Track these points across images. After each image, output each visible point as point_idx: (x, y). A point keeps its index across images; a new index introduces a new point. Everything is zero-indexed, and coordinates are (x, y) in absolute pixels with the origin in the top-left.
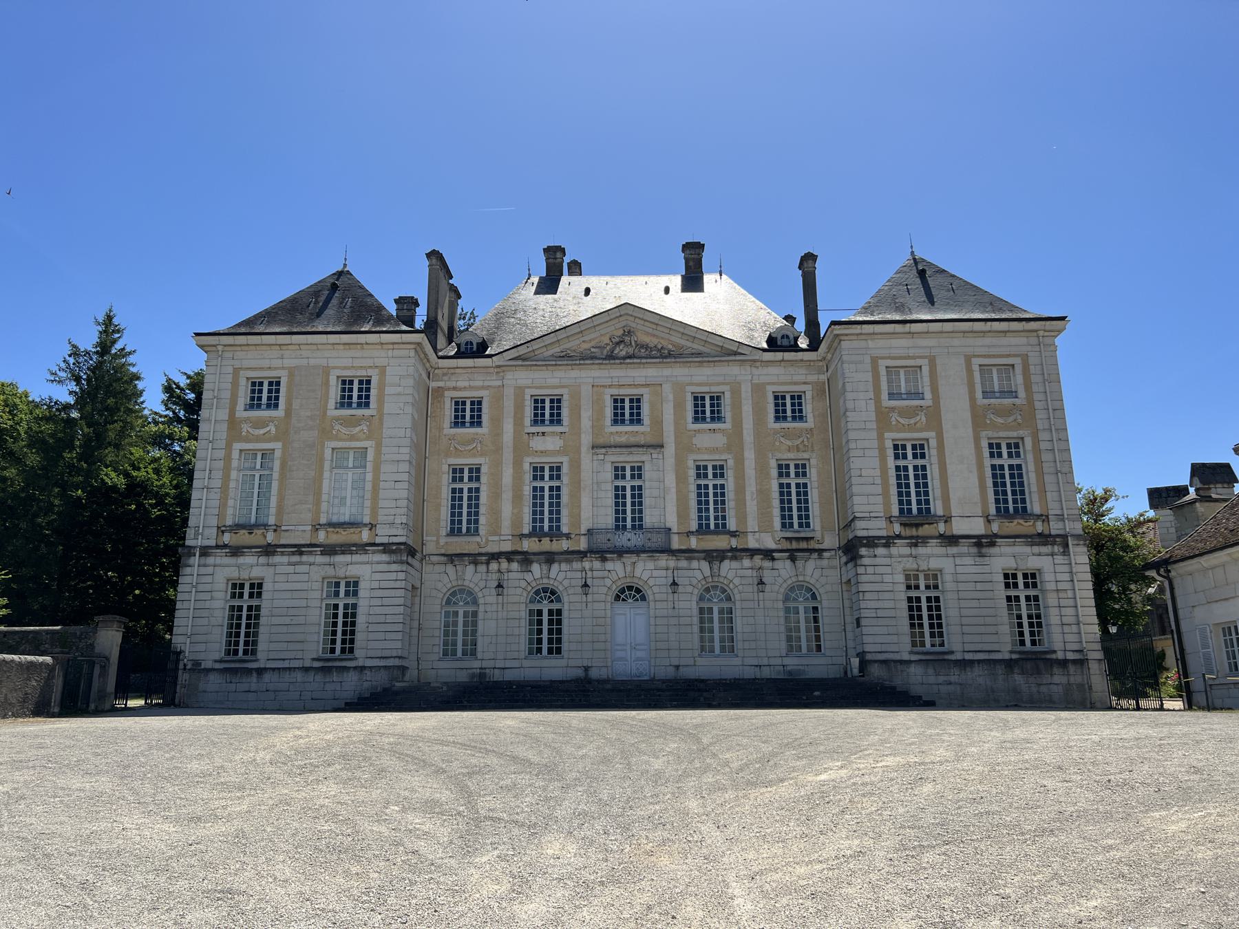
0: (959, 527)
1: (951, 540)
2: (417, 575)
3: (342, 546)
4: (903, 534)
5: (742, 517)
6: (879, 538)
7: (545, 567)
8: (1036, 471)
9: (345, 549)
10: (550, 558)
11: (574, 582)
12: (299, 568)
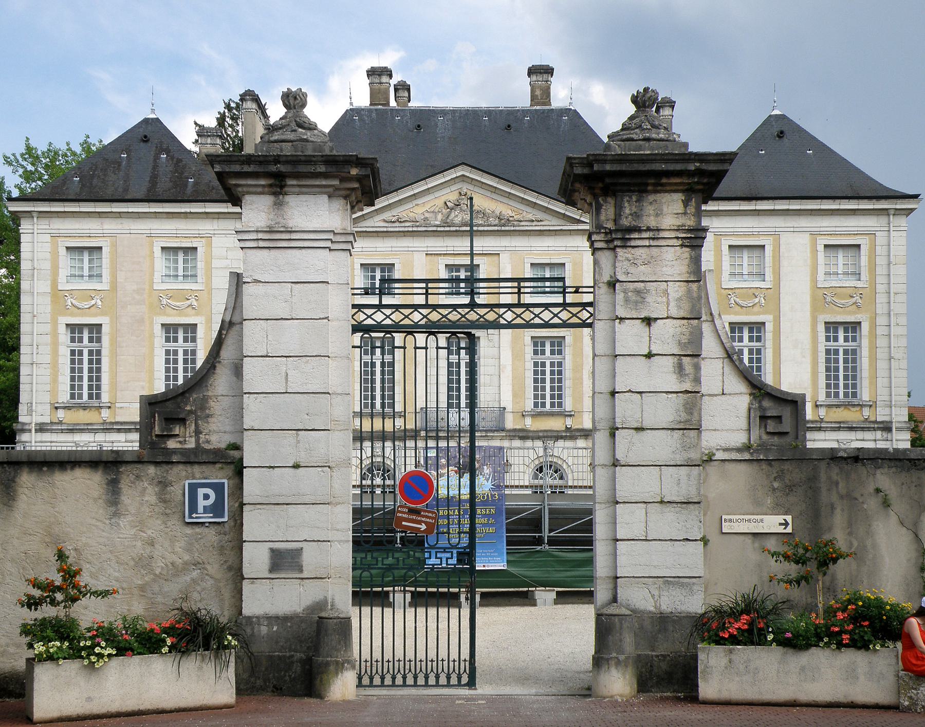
5: (578, 399)
8: (870, 357)
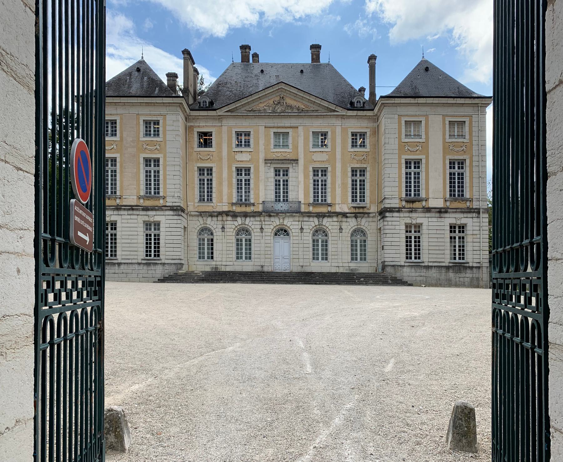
0: (432, 203)
1: (428, 210)
2: (186, 221)
3: (151, 207)
4: (406, 207)
6: (395, 208)
7: (243, 219)
9: (153, 209)
10: (245, 215)
11: (256, 227)
12: (132, 217)
